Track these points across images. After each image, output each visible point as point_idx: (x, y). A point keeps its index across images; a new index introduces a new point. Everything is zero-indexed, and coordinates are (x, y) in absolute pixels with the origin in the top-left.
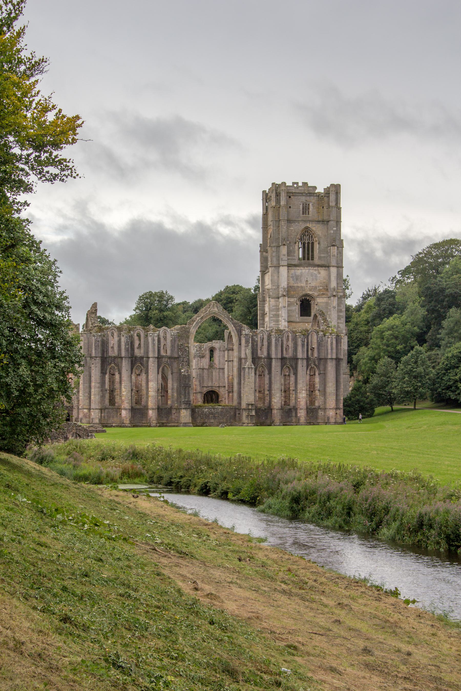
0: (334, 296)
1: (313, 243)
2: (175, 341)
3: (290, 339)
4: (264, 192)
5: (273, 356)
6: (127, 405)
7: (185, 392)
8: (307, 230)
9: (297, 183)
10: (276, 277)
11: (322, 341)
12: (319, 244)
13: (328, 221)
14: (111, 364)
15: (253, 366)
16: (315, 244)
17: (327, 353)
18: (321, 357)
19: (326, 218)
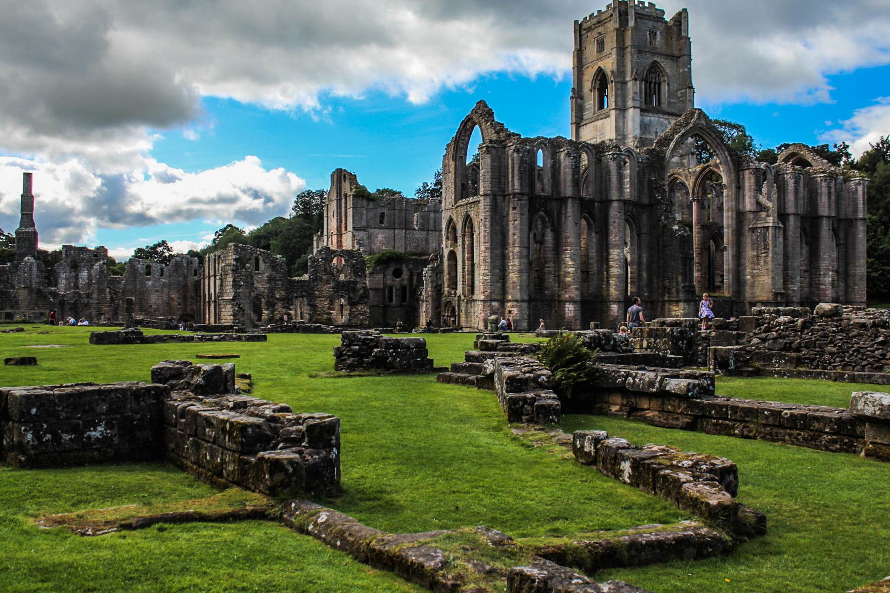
0: (693, 154)
1: (659, 84)
2: (644, 174)
3: (801, 185)
4: (576, 22)
5: (791, 209)
6: (576, 292)
7: (685, 269)
8: (655, 64)
9: (643, 3)
10: (621, 124)
11: (842, 190)
12: (668, 85)
13: (679, 57)
14: (539, 211)
15: (781, 225)
16: (663, 84)
17: (856, 211)
18: (842, 216)
19: (676, 53)
